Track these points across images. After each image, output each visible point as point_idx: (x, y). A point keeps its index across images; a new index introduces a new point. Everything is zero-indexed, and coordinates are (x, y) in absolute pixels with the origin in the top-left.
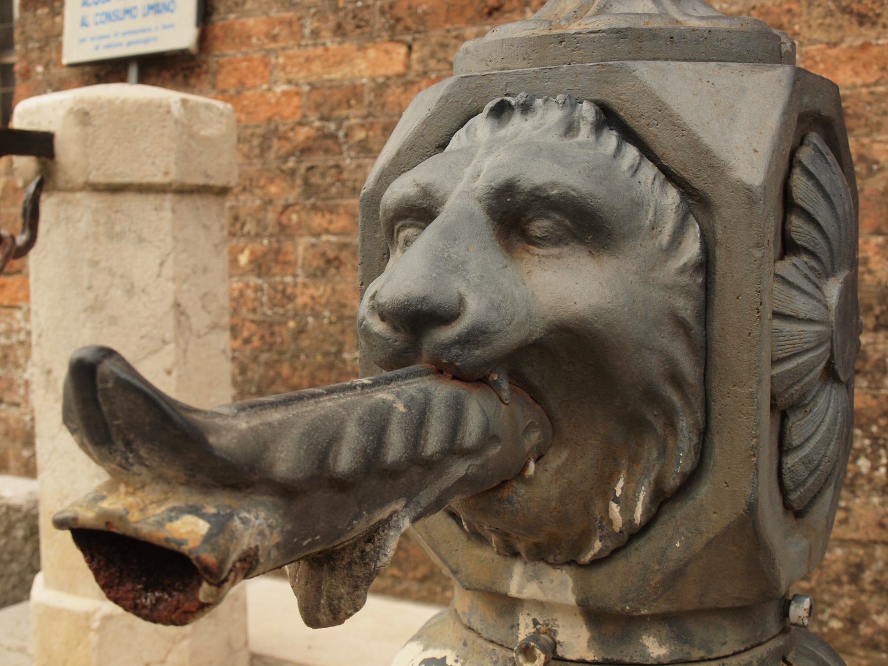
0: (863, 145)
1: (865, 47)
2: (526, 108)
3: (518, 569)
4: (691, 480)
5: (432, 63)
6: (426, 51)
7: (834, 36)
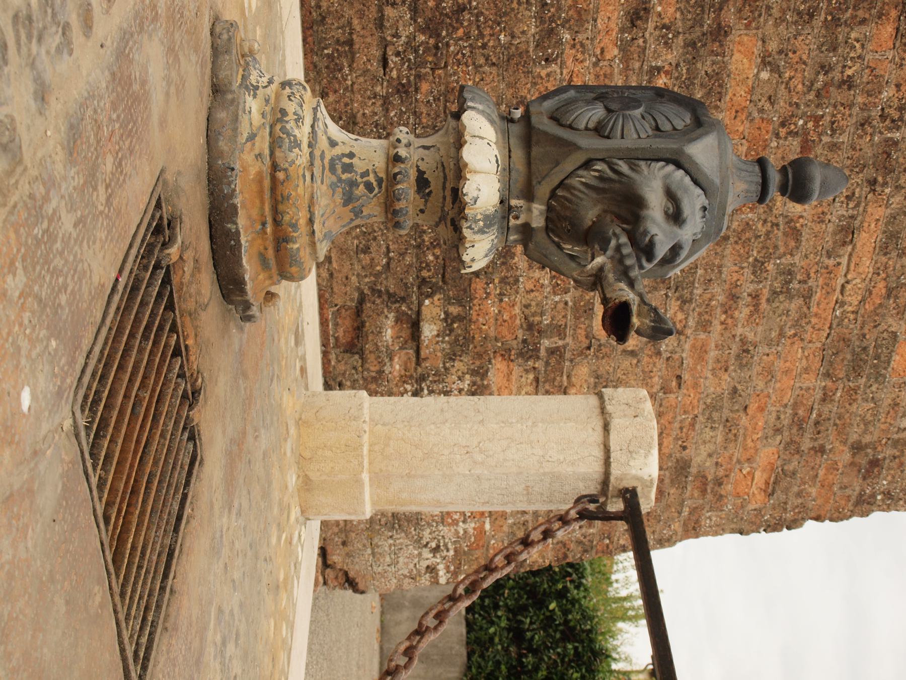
2: (704, 217)
3: (543, 207)
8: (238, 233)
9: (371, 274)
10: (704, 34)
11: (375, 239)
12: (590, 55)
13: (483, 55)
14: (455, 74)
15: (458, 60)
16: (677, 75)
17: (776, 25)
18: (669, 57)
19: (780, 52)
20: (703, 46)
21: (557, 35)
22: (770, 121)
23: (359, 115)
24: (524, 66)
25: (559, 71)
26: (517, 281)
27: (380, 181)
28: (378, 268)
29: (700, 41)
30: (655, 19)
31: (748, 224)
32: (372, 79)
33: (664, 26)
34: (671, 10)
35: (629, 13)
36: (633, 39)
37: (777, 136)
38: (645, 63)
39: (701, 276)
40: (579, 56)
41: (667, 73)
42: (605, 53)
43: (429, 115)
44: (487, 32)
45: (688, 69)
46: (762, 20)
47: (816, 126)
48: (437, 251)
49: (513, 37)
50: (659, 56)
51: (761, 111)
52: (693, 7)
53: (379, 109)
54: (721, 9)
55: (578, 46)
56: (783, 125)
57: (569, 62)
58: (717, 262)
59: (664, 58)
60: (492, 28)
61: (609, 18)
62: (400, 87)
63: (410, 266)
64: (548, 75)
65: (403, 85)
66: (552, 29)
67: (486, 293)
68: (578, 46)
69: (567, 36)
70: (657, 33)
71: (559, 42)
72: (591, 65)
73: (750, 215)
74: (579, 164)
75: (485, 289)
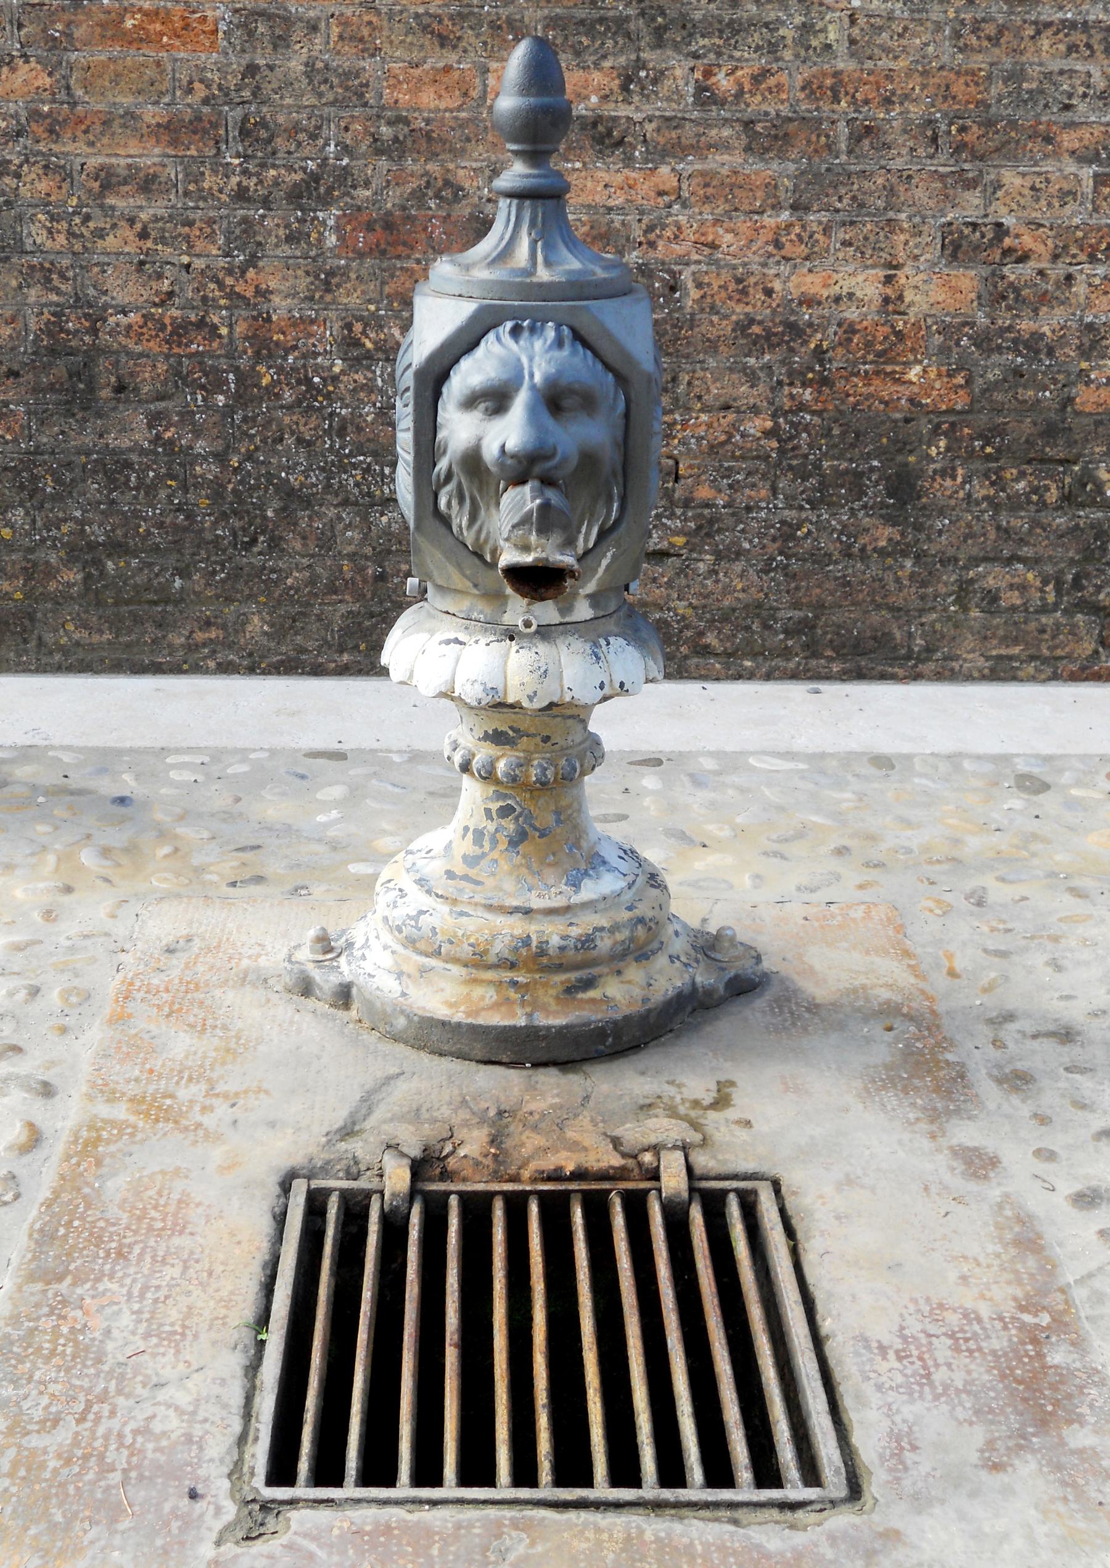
0: (448, 170)
1: (447, 69)
7: (416, 55)
10: (643, 14)
12: (669, 215)
14: (684, 442)
16: (712, 56)
18: (678, 72)
20: (663, 14)
24: (681, 328)
25: (693, 268)
26: (1090, 327)
29: (653, 19)
32: (686, 576)
33: (625, 88)
34: (597, 77)
35: (600, 152)
38: (687, 116)
40: (668, 233)
41: (708, 73)
42: (667, 188)
45: (703, 36)
48: (1011, 473)
57: (678, 249)
59: (681, 83)
61: (606, 186)
62: (704, 531)
64: (699, 285)
65: (699, 528)
69: (633, 257)
70: (636, 98)
71: (644, 270)
72: (686, 212)
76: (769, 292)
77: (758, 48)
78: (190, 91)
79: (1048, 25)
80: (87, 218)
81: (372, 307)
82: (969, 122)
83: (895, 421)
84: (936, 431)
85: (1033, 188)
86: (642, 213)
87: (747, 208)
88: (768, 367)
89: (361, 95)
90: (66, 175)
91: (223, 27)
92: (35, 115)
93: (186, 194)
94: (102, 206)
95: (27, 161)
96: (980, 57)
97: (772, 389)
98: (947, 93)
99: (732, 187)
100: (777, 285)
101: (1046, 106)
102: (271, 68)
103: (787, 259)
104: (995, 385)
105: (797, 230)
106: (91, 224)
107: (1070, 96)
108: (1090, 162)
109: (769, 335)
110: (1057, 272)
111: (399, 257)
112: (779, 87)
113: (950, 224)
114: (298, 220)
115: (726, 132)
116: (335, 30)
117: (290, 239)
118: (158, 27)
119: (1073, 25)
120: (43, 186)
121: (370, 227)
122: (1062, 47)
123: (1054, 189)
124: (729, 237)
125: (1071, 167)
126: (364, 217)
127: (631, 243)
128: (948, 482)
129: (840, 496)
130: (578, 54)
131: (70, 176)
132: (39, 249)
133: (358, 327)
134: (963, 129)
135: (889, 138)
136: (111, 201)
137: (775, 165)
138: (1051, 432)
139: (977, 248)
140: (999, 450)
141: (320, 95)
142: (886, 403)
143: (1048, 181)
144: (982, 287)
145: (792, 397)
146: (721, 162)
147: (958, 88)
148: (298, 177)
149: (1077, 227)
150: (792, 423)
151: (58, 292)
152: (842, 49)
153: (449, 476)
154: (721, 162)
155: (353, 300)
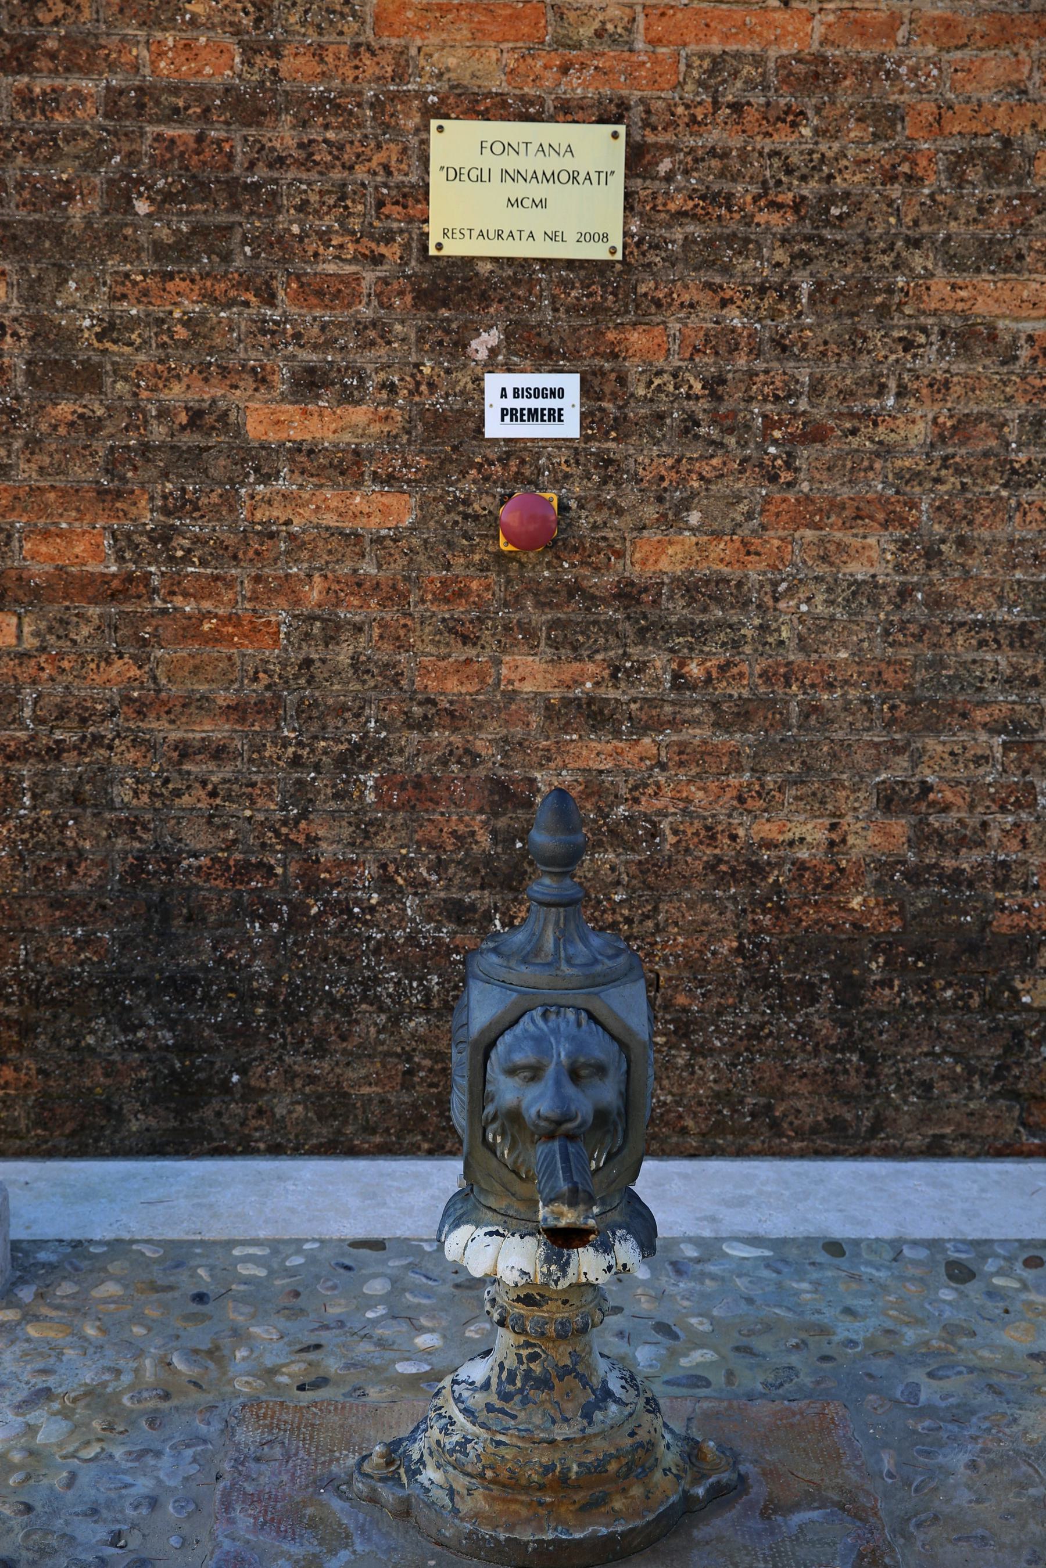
1: (468, 661)
4: (620, 1149)
5: (51, 639)
6: (43, 625)
7: (443, 651)
8: (540, 1542)
9: (968, 1080)
10: (628, 618)
11: (909, 1073)
12: (650, 776)
13: (641, 922)
14: (665, 959)
15: (647, 955)
17: (620, 512)
18: (658, 664)
19: (660, 500)
21: (618, 824)
22: (767, 500)
23: (716, 1087)
27: (528, 1345)
28: (959, 1069)
29: (637, 622)
30: (603, 690)
31: (939, 508)
33: (614, 676)
34: (591, 667)
36: (630, 719)
37: (790, 485)
39: (1025, 573)
41: (682, 664)
43: (723, 994)
44: (609, 918)
46: (611, 535)
47: (780, 424)
48: (939, 983)
49: (618, 883)
50: (657, 678)
51: (749, 516)
52: (589, 637)
53: (709, 1063)
54: (593, 597)
55: (636, 794)
56: (774, 478)
57: (658, 804)
58: (1003, 550)
60: (604, 912)
63: (959, 1024)
64: (675, 832)
65: (677, 1029)
66: (610, 831)
67: (1019, 911)
68: (636, 794)
70: (623, 685)
71: (630, 820)
73: (924, 507)
74: (489, 1154)
75: (1012, 912)
76: (734, 838)
77: (724, 644)
78: (255, 679)
79: (962, 624)
80: (167, 781)
81: (404, 851)
82: (898, 702)
83: (841, 941)
84: (876, 949)
85: (952, 753)
86: (628, 775)
87: (714, 770)
88: (733, 898)
89: (396, 683)
90: (151, 747)
91: (284, 629)
92: (127, 700)
93: (251, 761)
94: (180, 772)
95: (118, 736)
96: (906, 650)
97: (737, 916)
98: (878, 678)
99: (703, 753)
100: (741, 832)
101: (962, 688)
102: (323, 661)
103: (750, 812)
104: (926, 912)
105: (757, 787)
106: (171, 786)
107: (982, 681)
108: (999, 734)
109: (734, 872)
110: (973, 822)
111: (427, 811)
112: (741, 675)
113: (883, 782)
114: (344, 782)
115: (697, 711)
116: (376, 632)
117: (337, 796)
118: (231, 629)
119: (982, 624)
120: (132, 756)
121: (402, 786)
122: (974, 642)
123: (969, 755)
124: (700, 794)
125: (983, 736)
126: (398, 778)
127: (618, 799)
128: (887, 992)
129: (795, 1003)
130: (575, 649)
131: (154, 747)
132: (126, 806)
133: (392, 868)
134: (893, 708)
135: (832, 715)
136: (186, 767)
137: (738, 736)
138: (972, 948)
139: (906, 801)
140: (928, 965)
141: (364, 682)
142: (834, 927)
143: (965, 748)
144: (911, 834)
145: (754, 922)
146: (695, 734)
147: (888, 675)
148: (343, 747)
149: (990, 785)
150: (755, 944)
151: (140, 840)
152: (793, 644)
153: (495, 1118)
154: (695, 734)
155: (389, 844)
